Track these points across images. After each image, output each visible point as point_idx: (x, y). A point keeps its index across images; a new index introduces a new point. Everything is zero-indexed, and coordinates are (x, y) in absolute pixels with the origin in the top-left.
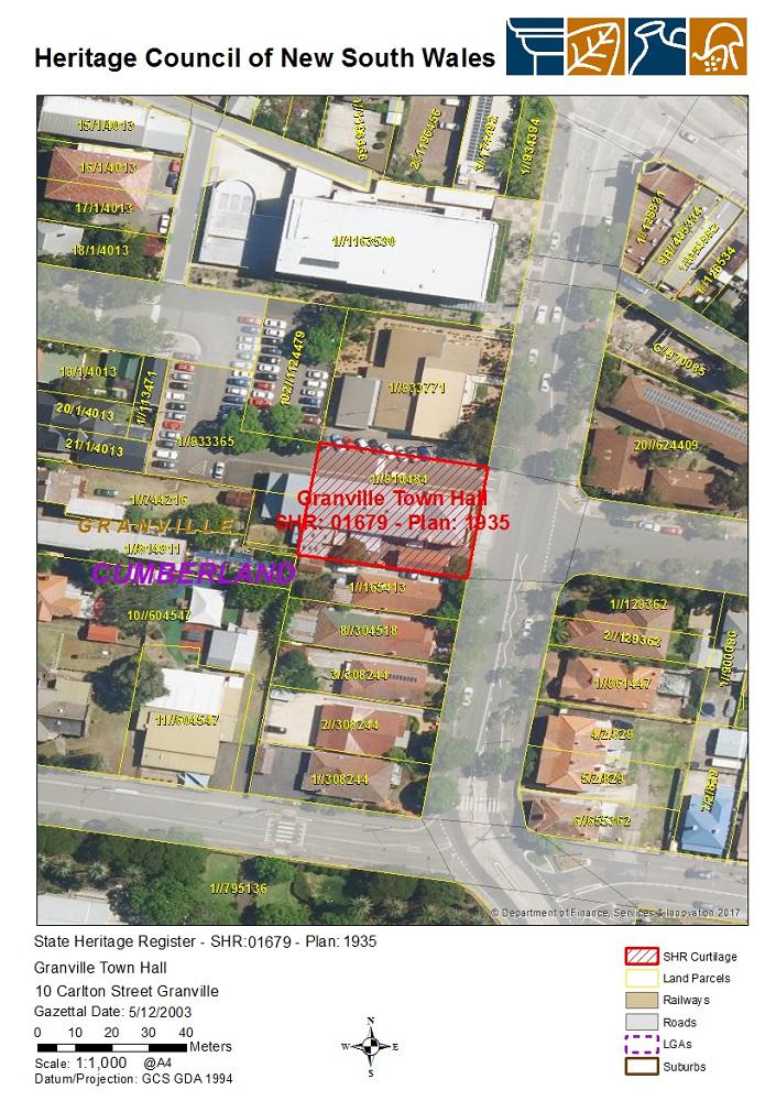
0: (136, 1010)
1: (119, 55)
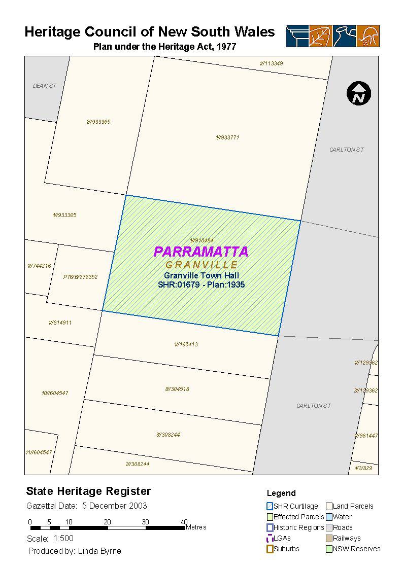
0: (64, 537)
1: (188, 46)
